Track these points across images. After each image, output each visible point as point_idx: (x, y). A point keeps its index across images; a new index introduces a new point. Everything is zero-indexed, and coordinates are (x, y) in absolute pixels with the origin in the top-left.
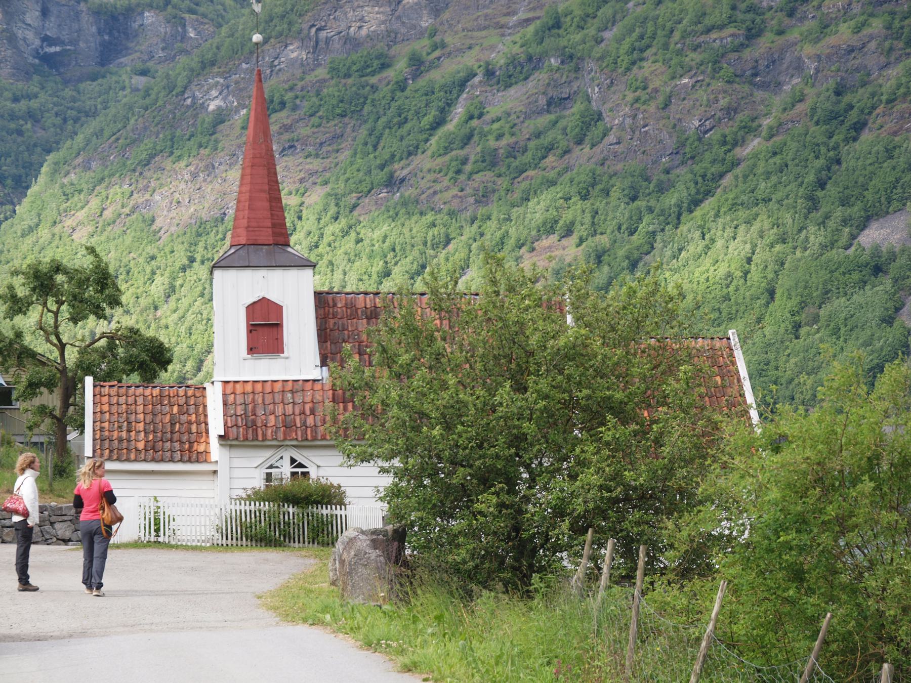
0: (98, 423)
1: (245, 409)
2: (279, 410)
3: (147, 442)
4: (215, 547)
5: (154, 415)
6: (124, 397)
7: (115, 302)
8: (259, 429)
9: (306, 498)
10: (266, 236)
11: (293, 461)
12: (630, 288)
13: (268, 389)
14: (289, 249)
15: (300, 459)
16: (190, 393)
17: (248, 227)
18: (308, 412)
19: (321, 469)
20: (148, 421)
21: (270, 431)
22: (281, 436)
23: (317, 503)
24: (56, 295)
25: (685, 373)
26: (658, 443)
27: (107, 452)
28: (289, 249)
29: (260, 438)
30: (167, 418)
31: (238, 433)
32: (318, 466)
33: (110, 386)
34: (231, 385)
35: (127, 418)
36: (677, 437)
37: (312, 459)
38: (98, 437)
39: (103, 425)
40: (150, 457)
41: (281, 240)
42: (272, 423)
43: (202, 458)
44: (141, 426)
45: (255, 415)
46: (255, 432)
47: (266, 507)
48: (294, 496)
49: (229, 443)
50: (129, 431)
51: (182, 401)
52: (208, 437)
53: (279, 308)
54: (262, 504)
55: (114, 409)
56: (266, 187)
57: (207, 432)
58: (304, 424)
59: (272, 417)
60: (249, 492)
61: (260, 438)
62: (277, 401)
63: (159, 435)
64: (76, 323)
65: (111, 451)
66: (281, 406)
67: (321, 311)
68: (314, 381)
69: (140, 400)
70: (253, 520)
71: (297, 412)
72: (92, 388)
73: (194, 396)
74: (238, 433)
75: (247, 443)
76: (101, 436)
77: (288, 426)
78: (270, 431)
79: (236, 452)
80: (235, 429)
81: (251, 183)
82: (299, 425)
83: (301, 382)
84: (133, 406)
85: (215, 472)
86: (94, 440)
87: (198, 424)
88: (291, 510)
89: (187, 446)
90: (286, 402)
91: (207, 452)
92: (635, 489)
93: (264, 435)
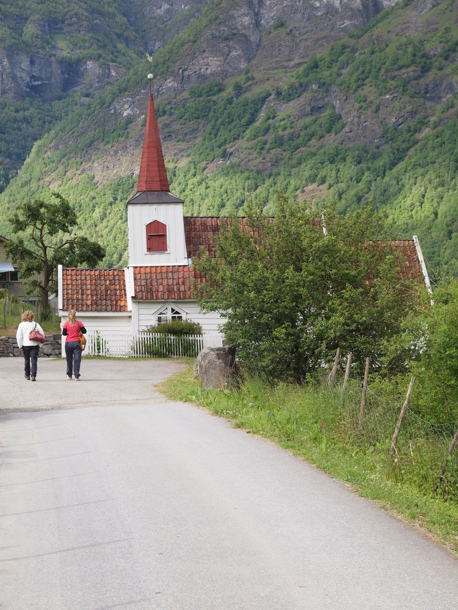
0: (65, 291)
1: (146, 282)
2: (165, 282)
3: (92, 300)
4: (131, 358)
5: (96, 286)
7: (73, 223)
9: (180, 331)
10: (156, 186)
11: (173, 310)
12: (358, 213)
13: (159, 271)
14: (170, 194)
15: (177, 309)
16: (116, 273)
17: (147, 181)
18: (181, 284)
19: (188, 315)
20: (93, 289)
21: (160, 294)
22: (166, 297)
23: (186, 333)
24: (41, 220)
25: (389, 259)
26: (375, 298)
27: (71, 306)
28: (170, 194)
29: (155, 298)
30: (103, 288)
31: (143, 295)
32: (187, 313)
33: (72, 270)
34: (138, 269)
35: (82, 287)
36: (386, 295)
37: (183, 309)
38: (65, 298)
40: (94, 309)
41: (165, 188)
42: (161, 290)
43: (123, 309)
44: (89, 292)
47: (158, 336)
48: (174, 330)
49: (138, 301)
50: (82, 295)
51: (111, 278)
52: (126, 297)
55: (74, 283)
56: (157, 159)
57: (125, 295)
58: (179, 290)
59: (161, 286)
60: (149, 328)
61: (155, 298)
62: (163, 277)
63: (99, 296)
64: (52, 235)
65: (73, 306)
66: (166, 280)
67: (188, 228)
68: (184, 266)
69: (88, 278)
71: (175, 283)
73: (118, 275)
74: (143, 295)
75: (147, 301)
76: (67, 297)
77: (170, 291)
78: (160, 294)
80: (141, 293)
81: (148, 157)
82: (176, 291)
83: (177, 267)
84: (85, 281)
85: (130, 317)
86: (63, 300)
87: (121, 290)
88: (172, 337)
89: (114, 303)
90: (169, 278)
91: (125, 306)
92: (362, 324)
93: (157, 296)
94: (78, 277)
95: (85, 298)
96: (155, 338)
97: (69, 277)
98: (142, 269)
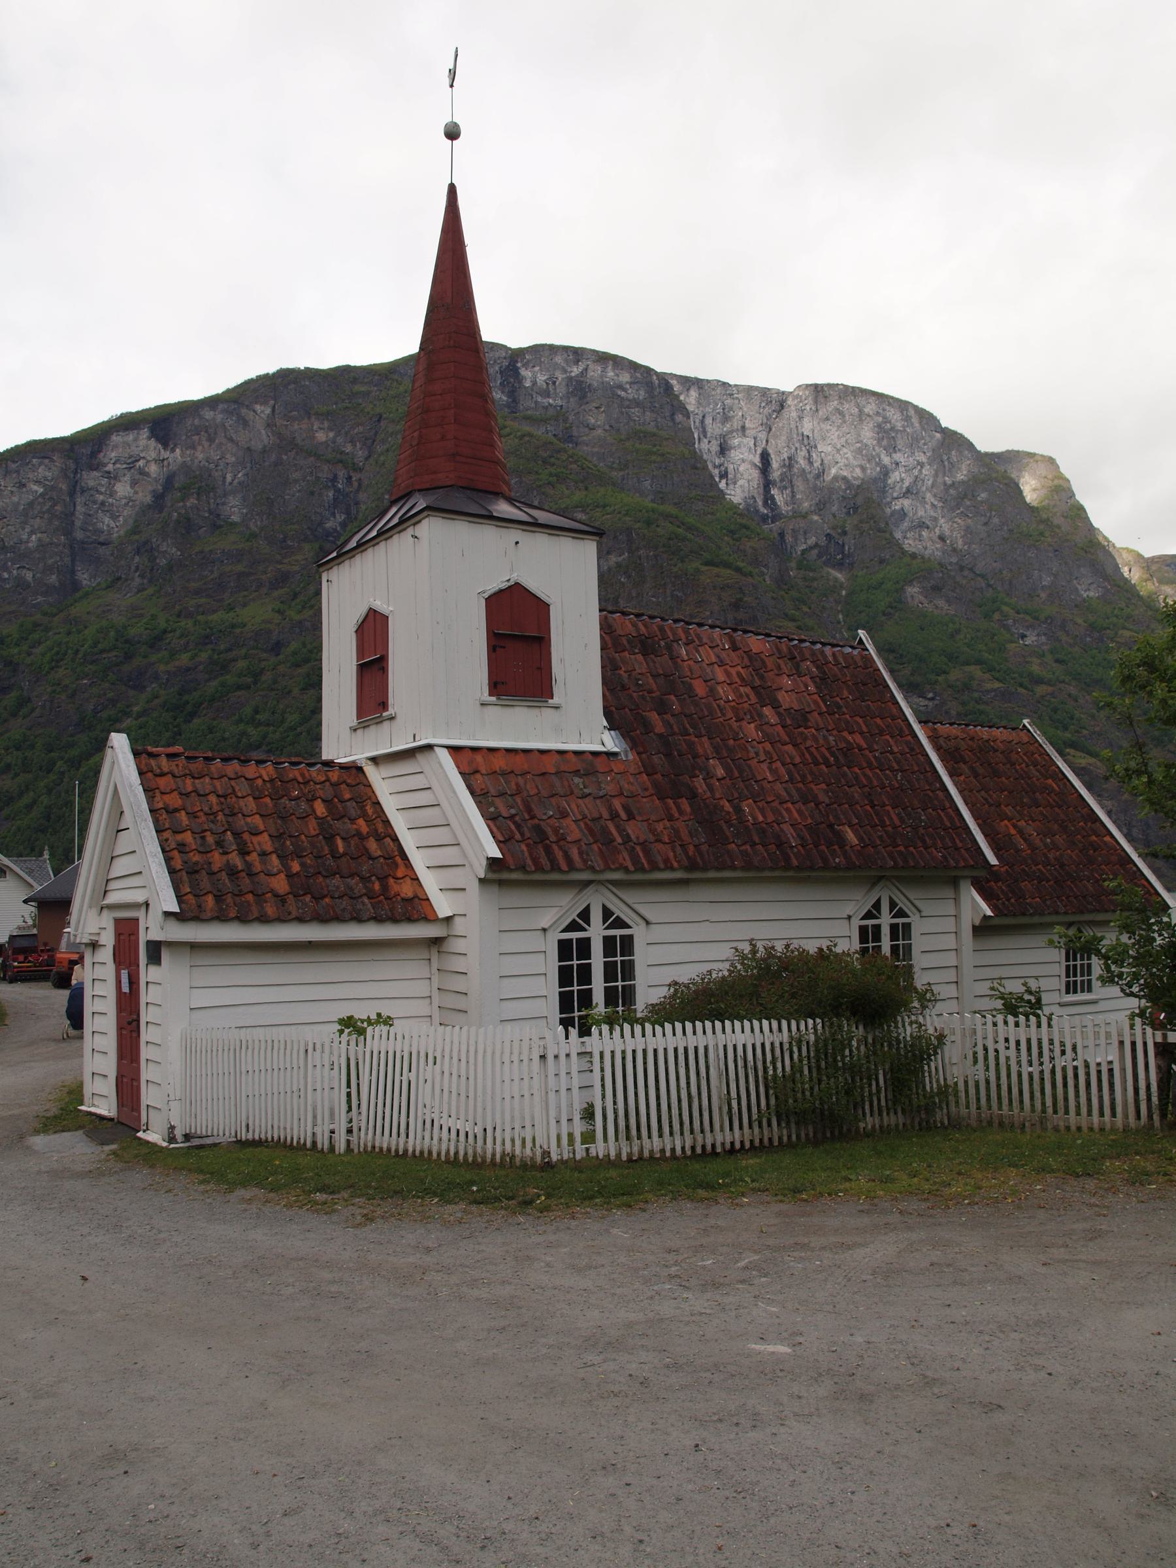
0: (167, 834)
3: (290, 876)
6: (207, 780)
8: (555, 847)
11: (607, 913)
15: (619, 911)
18: (623, 815)
22: (598, 863)
27: (210, 901)
30: (312, 827)
32: (648, 923)
33: (171, 756)
38: (178, 864)
39: (179, 837)
44: (265, 842)
45: (533, 817)
46: (548, 850)
47: (810, 1028)
49: (505, 876)
50: (244, 852)
53: (541, 608)
54: (802, 1024)
58: (627, 839)
61: (565, 868)
65: (219, 898)
69: (242, 788)
70: (788, 1068)
71: (606, 815)
72: (131, 757)
85: (437, 942)
87: (379, 839)
89: (377, 886)
94: (205, 784)
95: (258, 867)
96: (799, 1042)
97: (162, 782)
98: (479, 758)
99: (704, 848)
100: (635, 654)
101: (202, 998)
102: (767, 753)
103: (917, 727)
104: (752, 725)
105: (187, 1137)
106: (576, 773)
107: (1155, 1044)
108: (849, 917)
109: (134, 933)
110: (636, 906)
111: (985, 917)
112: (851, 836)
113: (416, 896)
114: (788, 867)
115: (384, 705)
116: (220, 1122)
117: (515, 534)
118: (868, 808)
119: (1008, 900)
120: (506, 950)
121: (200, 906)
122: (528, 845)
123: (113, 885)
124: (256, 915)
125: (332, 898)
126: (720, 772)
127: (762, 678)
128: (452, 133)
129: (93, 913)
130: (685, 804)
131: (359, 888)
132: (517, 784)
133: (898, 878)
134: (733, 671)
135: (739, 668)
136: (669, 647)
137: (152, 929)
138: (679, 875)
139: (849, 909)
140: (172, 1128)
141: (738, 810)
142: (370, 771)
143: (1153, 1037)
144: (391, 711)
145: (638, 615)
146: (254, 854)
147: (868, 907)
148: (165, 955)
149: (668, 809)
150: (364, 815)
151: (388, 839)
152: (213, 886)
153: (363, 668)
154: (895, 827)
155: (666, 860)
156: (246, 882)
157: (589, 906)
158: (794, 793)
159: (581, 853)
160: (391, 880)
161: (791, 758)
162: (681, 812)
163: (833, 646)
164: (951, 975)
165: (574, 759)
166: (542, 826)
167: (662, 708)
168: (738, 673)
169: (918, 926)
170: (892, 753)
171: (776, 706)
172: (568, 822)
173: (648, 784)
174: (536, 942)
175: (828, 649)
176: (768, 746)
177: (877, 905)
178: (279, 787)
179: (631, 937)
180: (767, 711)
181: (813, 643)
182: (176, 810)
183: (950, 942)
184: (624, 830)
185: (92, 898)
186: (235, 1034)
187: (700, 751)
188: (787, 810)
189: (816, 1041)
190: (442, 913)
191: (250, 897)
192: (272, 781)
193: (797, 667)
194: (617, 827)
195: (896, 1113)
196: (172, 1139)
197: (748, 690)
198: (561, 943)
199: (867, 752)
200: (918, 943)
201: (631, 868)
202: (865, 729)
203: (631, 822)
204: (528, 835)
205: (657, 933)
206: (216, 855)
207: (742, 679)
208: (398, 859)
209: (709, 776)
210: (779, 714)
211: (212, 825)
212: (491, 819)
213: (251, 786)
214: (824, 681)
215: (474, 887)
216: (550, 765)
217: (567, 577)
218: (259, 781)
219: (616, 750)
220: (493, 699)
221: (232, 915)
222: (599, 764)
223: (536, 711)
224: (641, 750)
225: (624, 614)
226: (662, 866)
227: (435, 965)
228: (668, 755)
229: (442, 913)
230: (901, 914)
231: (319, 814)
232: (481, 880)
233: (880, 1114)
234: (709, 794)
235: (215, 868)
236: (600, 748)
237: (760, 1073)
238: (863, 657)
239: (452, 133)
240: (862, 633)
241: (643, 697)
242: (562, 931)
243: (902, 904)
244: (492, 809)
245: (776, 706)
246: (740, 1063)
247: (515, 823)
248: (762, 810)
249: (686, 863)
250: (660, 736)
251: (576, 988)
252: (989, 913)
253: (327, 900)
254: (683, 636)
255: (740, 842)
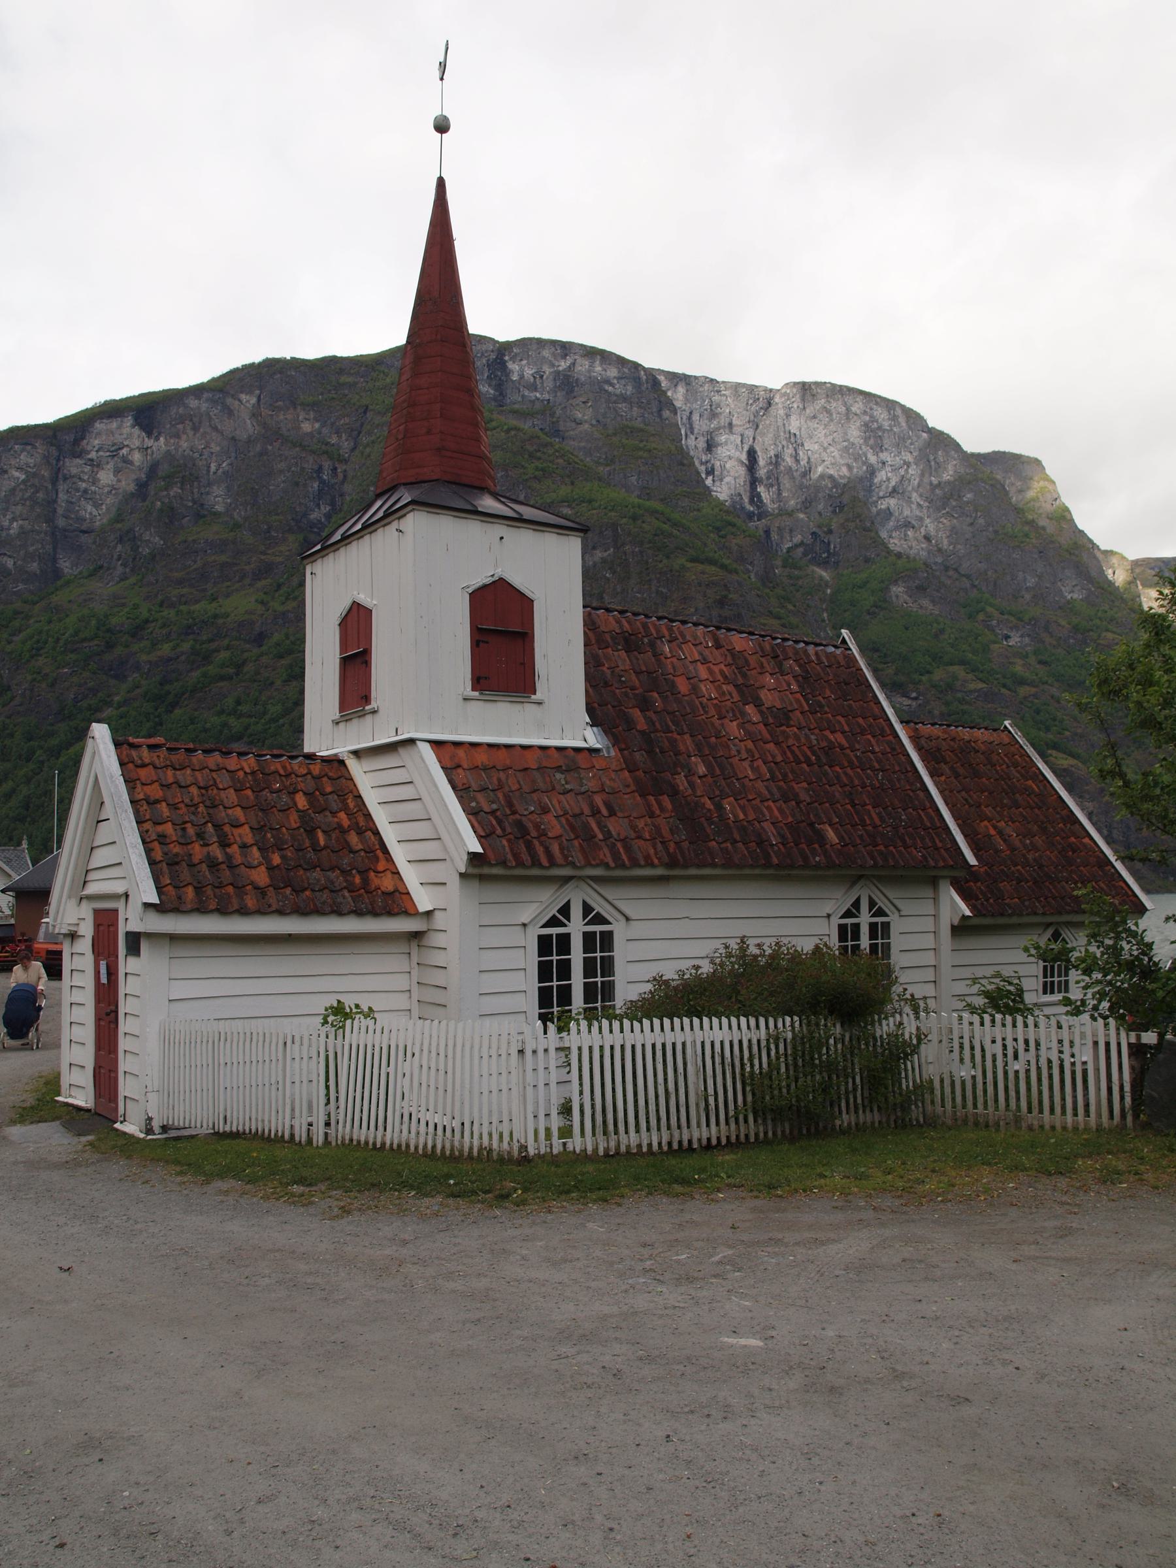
3: (271, 869)
6: (189, 771)
8: (536, 842)
11: (587, 909)
15: (599, 907)
18: (605, 812)
22: (578, 857)
27: (190, 891)
30: (294, 820)
32: (628, 919)
33: (152, 747)
38: (158, 855)
39: (160, 828)
44: (245, 834)
45: (514, 813)
46: (529, 846)
47: (788, 1026)
49: (486, 870)
50: (224, 844)
53: (525, 604)
58: (608, 835)
59: (546, 818)
61: (545, 863)
65: (198, 890)
68: (591, 751)
69: (223, 780)
70: (765, 1065)
71: (587, 811)
72: (112, 747)
79: (495, 892)
85: (417, 936)
87: (360, 833)
89: (358, 880)
94: (186, 776)
95: (238, 859)
97: (143, 773)
98: (461, 752)
99: (686, 845)
100: (618, 650)
101: (180, 990)
102: (748, 751)
103: (898, 727)
104: (735, 723)
105: (165, 1129)
106: (558, 769)
107: (1129, 1044)
108: (829, 916)
109: (114, 924)
110: (616, 903)
111: (964, 917)
112: (831, 835)
113: (396, 890)
114: (768, 865)
115: (367, 699)
116: (197, 1114)
117: (500, 529)
118: (849, 807)
119: (987, 900)
120: (485, 945)
121: (180, 898)
122: (509, 841)
123: (92, 876)
124: (236, 907)
125: (313, 890)
126: (702, 770)
127: (744, 676)
128: (442, 127)
129: (73, 902)
130: (667, 802)
131: (340, 881)
132: (499, 780)
133: (880, 879)
134: (716, 669)
135: (722, 666)
136: (652, 645)
137: (132, 920)
138: (660, 871)
139: (828, 907)
140: (150, 1119)
141: (719, 807)
142: (352, 764)
143: (1127, 1039)
144: (373, 705)
145: (621, 612)
146: (235, 847)
147: (847, 905)
148: (144, 946)
149: (649, 805)
150: (345, 808)
151: (369, 833)
152: (193, 877)
153: (346, 662)
154: (875, 827)
155: (647, 858)
156: (226, 875)
157: (569, 901)
158: (775, 790)
159: (562, 849)
160: (372, 874)
161: (773, 757)
162: (662, 809)
163: (816, 645)
164: (930, 975)
165: (556, 754)
166: (523, 822)
167: (645, 705)
168: (721, 672)
169: (897, 925)
170: (873, 752)
171: (758, 704)
172: (549, 818)
173: (630, 780)
174: (516, 937)
175: (811, 648)
176: (750, 745)
177: (857, 904)
178: (261, 780)
179: (611, 933)
180: (750, 709)
181: (796, 642)
182: (157, 802)
183: (928, 941)
184: (605, 826)
185: (71, 889)
186: (210, 1025)
187: (682, 748)
188: (768, 808)
189: (794, 1038)
190: (423, 905)
191: (230, 889)
192: (253, 773)
193: (780, 665)
194: (599, 824)
195: (872, 1111)
196: (149, 1131)
197: (731, 688)
198: (540, 937)
199: (848, 751)
200: (897, 942)
201: (612, 865)
202: (846, 728)
203: (612, 819)
204: (509, 830)
205: (637, 929)
206: (197, 846)
207: (725, 677)
208: (379, 853)
209: (690, 773)
210: (761, 712)
211: (193, 817)
212: (472, 813)
213: (232, 779)
214: (805, 679)
215: (454, 882)
216: (532, 761)
217: (551, 573)
218: (241, 773)
219: (598, 746)
220: (476, 694)
221: (212, 907)
222: (581, 759)
223: (518, 707)
224: (623, 746)
225: (608, 610)
226: (642, 863)
227: (415, 959)
228: (650, 752)
229: (423, 905)
230: (881, 913)
231: (300, 806)
232: (461, 875)
233: (856, 1112)
234: (690, 791)
235: (196, 860)
236: (582, 744)
237: (738, 1070)
238: (845, 657)
239: (442, 127)
240: (845, 633)
241: (626, 694)
242: (544, 926)
243: (881, 903)
244: (474, 804)
245: (758, 704)
246: (718, 1060)
247: (496, 818)
248: (743, 808)
249: (666, 859)
250: (642, 733)
251: (555, 983)
252: (968, 913)
253: (307, 893)
254: (666, 633)
255: (720, 840)
